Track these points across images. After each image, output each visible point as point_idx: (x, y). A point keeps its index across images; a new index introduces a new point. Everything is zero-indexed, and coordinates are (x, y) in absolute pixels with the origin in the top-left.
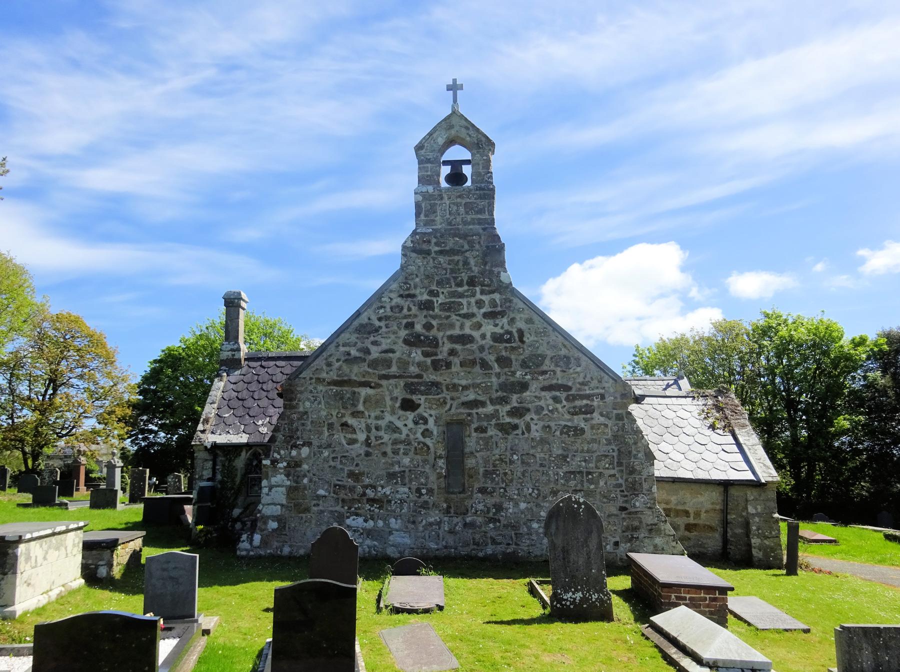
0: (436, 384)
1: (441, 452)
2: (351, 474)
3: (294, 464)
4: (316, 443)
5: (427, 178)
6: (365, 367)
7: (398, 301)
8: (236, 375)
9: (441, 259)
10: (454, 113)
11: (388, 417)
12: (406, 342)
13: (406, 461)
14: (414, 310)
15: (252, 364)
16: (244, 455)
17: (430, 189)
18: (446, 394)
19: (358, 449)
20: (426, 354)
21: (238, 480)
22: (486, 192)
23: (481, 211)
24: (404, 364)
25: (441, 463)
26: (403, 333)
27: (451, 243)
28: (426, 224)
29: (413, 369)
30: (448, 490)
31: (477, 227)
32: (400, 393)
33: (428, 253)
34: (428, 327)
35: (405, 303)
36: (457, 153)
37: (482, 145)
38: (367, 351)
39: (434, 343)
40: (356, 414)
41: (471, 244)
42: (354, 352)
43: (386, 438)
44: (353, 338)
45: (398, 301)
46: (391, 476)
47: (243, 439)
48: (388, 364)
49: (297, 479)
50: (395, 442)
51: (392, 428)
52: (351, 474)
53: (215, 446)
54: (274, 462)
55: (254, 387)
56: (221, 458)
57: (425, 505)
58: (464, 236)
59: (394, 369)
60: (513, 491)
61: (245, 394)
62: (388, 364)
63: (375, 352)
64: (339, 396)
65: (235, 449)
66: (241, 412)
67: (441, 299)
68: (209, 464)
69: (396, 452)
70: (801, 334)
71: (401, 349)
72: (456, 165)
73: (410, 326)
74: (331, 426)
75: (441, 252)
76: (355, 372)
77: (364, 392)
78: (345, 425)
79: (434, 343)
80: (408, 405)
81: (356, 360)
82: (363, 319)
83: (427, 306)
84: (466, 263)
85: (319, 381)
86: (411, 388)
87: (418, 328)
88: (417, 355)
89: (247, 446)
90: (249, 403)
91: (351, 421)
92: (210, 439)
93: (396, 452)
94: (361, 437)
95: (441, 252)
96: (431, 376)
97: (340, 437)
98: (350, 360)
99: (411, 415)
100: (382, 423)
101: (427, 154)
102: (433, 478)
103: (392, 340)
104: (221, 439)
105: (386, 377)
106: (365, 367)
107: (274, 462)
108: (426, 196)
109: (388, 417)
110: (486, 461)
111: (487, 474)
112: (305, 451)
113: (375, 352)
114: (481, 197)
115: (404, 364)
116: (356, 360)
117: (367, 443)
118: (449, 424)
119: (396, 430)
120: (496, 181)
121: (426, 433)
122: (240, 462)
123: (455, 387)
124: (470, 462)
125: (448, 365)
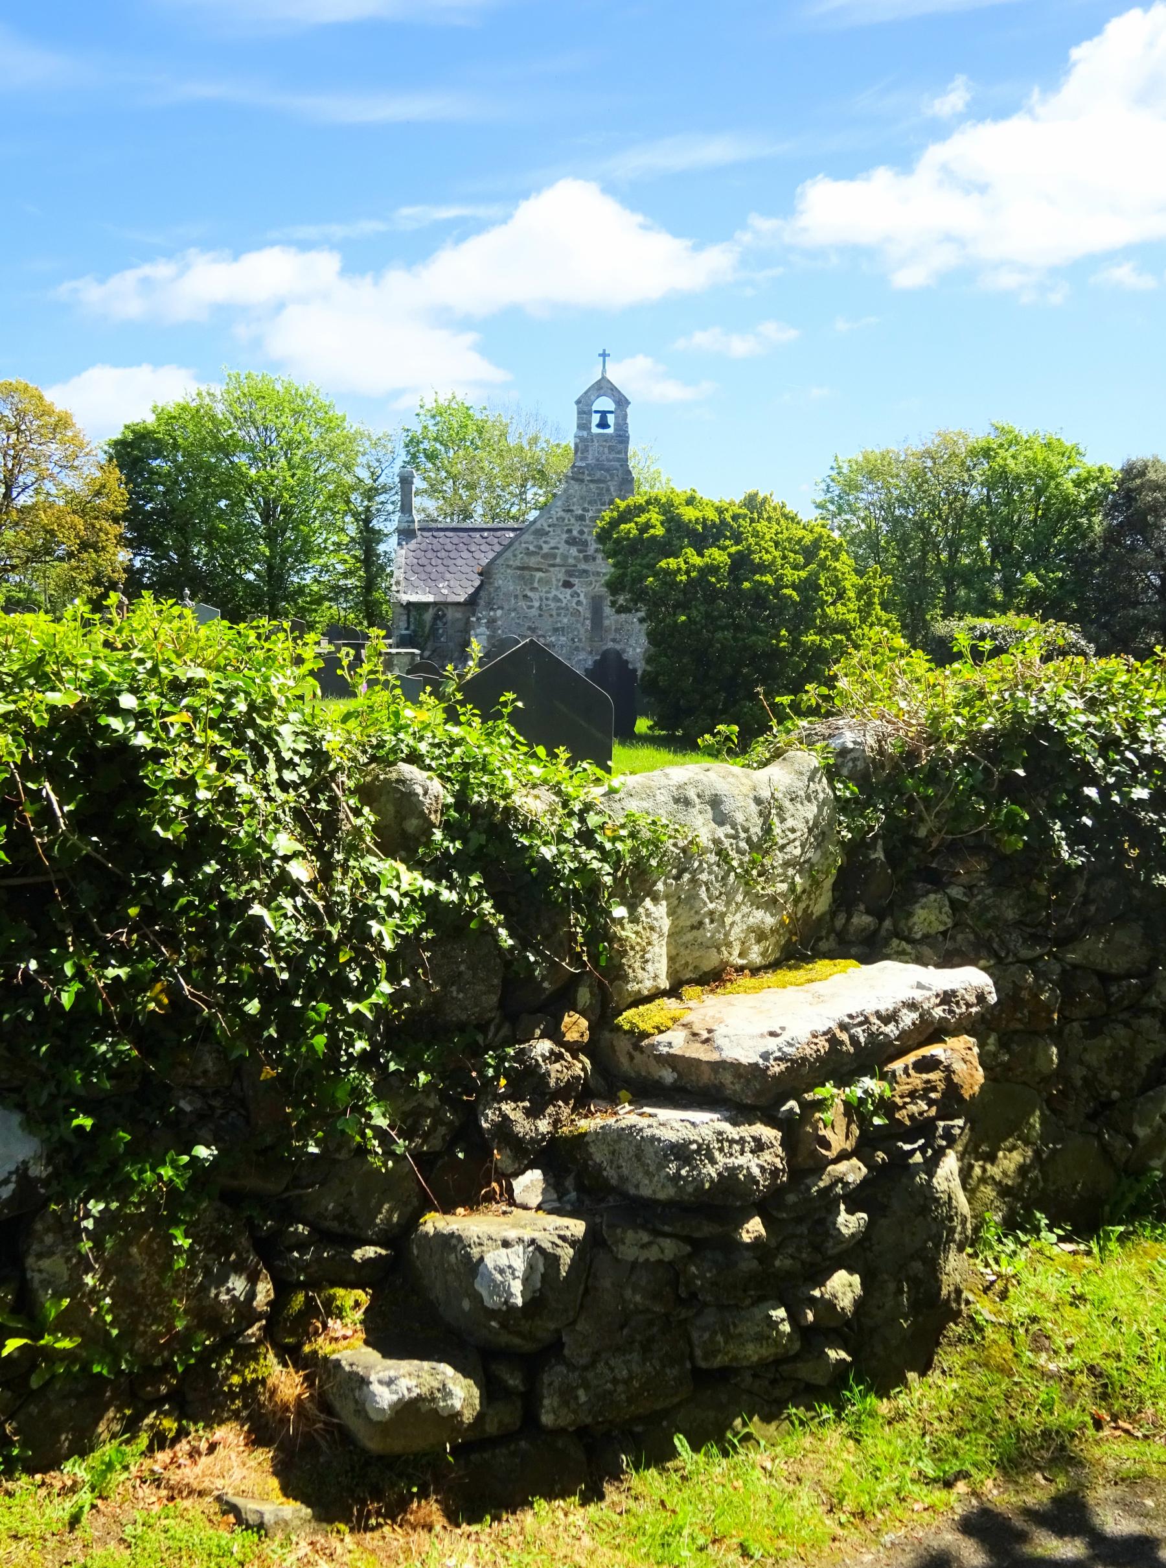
0: (585, 571)
1: (588, 615)
2: (529, 628)
3: (492, 622)
4: (506, 607)
5: (583, 426)
6: (539, 559)
7: (561, 514)
8: (413, 544)
9: (592, 486)
10: (603, 378)
11: (554, 592)
12: (567, 542)
13: (565, 620)
14: (573, 521)
15: (425, 534)
16: (431, 611)
17: (585, 434)
18: (592, 578)
19: (534, 612)
20: (580, 551)
21: (427, 629)
22: (622, 438)
23: (619, 452)
24: (565, 557)
25: (588, 622)
26: (565, 536)
27: (598, 474)
28: (582, 459)
29: (571, 561)
30: (591, 640)
31: (617, 464)
32: (562, 576)
33: (582, 481)
34: (581, 532)
35: (567, 516)
36: (605, 403)
37: (622, 402)
38: (541, 548)
39: (585, 544)
40: (533, 589)
41: (612, 476)
42: (531, 548)
43: (553, 605)
44: (531, 538)
45: (561, 514)
46: (556, 630)
47: (430, 598)
48: (554, 556)
49: (494, 630)
50: (559, 608)
51: (556, 599)
52: (529, 628)
53: (409, 603)
54: (479, 619)
55: (430, 554)
56: (413, 613)
57: (577, 649)
58: (607, 470)
59: (558, 560)
60: (632, 642)
61: (423, 561)
62: (554, 556)
63: (546, 549)
64: (521, 577)
65: (425, 606)
66: (424, 576)
67: (591, 514)
68: (405, 618)
69: (559, 615)
70: (1016, 467)
71: (563, 547)
72: (604, 414)
73: (569, 531)
74: (516, 597)
75: (591, 481)
76: (533, 561)
77: (539, 575)
78: (525, 596)
79: (585, 544)
80: (567, 585)
81: (533, 553)
82: (538, 525)
83: (581, 518)
84: (608, 490)
85: (508, 566)
86: (570, 573)
87: (575, 533)
88: (574, 551)
89: (435, 604)
90: (429, 568)
91: (529, 594)
92: (405, 598)
93: (559, 615)
94: (537, 604)
95: (591, 481)
96: (583, 566)
97: (522, 604)
98: (529, 553)
99: (569, 591)
100: (550, 596)
101: (584, 407)
102: (582, 631)
103: (557, 540)
104: (414, 598)
105: (553, 566)
106: (539, 559)
107: (479, 619)
108: (582, 439)
109: (554, 592)
110: (617, 621)
111: (617, 630)
112: (499, 613)
113: (546, 549)
114: (621, 442)
115: (565, 557)
116: (533, 553)
117: (540, 608)
118: (593, 598)
119: (560, 600)
120: (631, 432)
121: (579, 603)
122: (428, 616)
123: (598, 574)
124: (606, 623)
125: (594, 559)
